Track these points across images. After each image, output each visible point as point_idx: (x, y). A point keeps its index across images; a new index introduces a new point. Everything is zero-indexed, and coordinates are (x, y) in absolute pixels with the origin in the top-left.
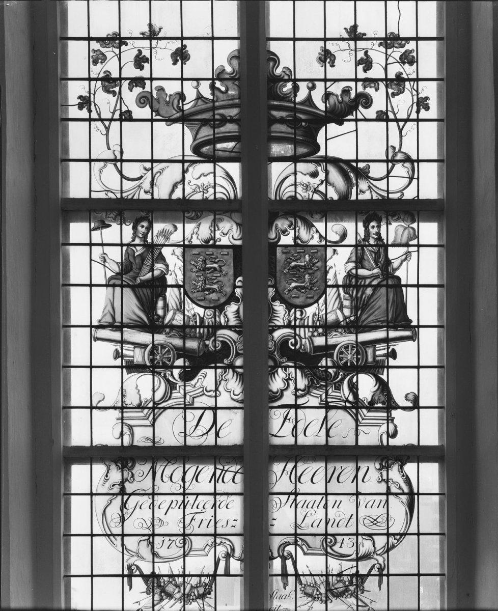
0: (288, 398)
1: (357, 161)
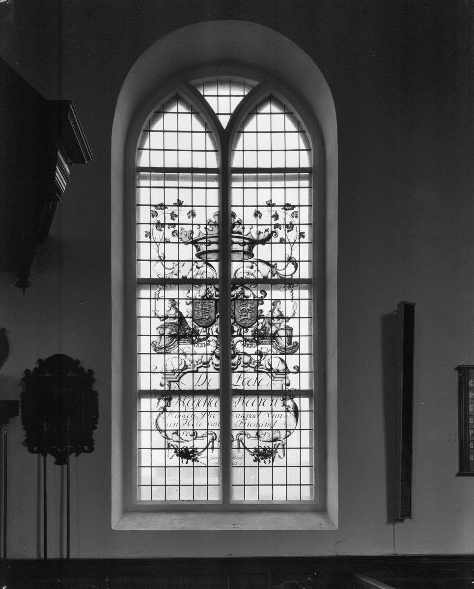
0: (240, 368)
1: (271, 261)
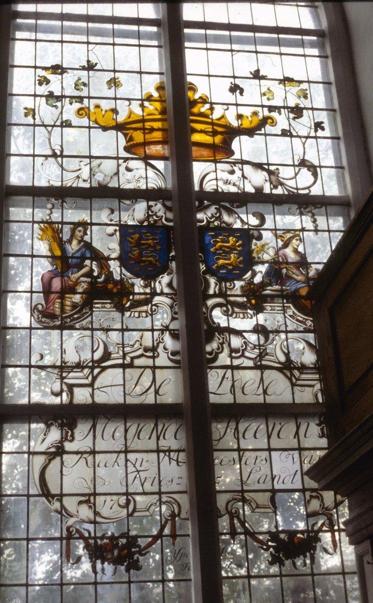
1: (268, 164)
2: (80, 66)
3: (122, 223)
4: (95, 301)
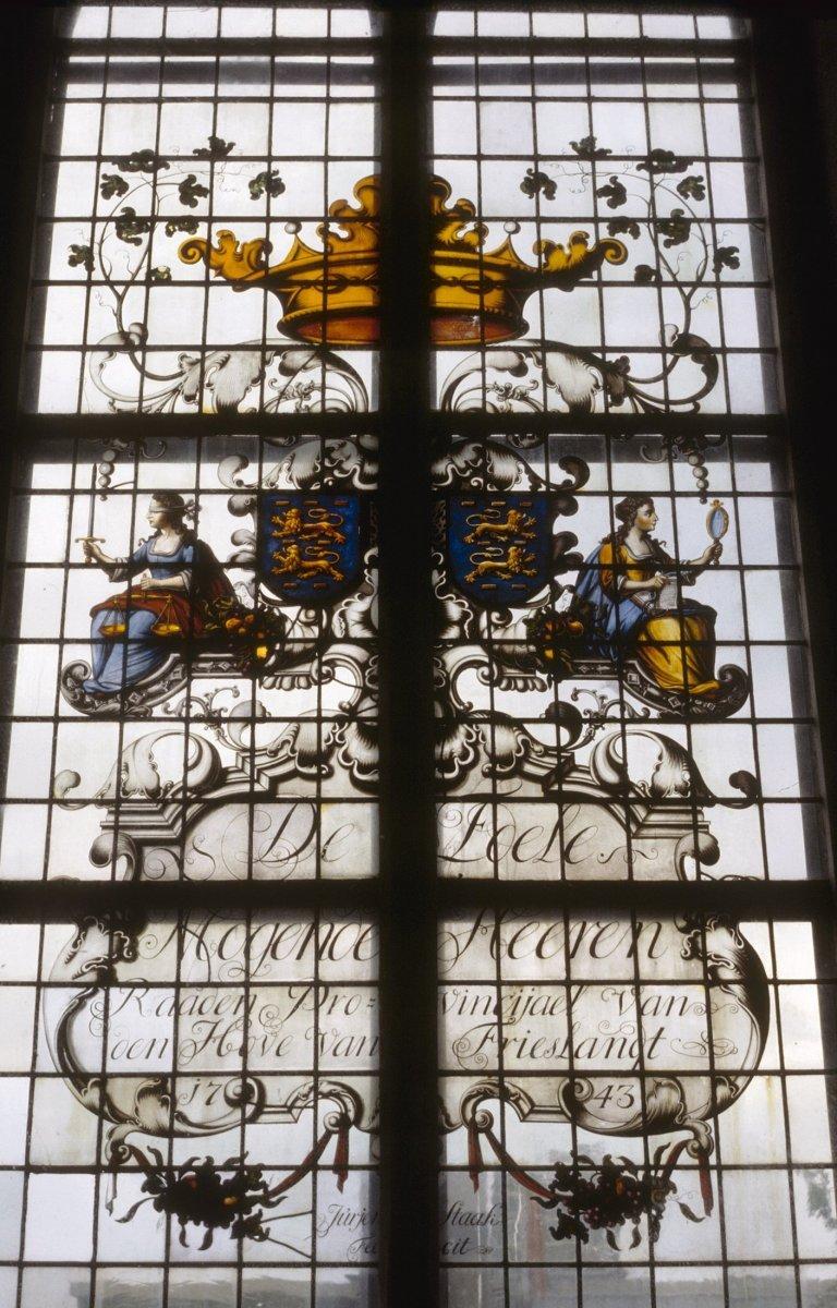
1: (604, 349)
2: (195, 151)
3: (264, 487)
4: (203, 655)
